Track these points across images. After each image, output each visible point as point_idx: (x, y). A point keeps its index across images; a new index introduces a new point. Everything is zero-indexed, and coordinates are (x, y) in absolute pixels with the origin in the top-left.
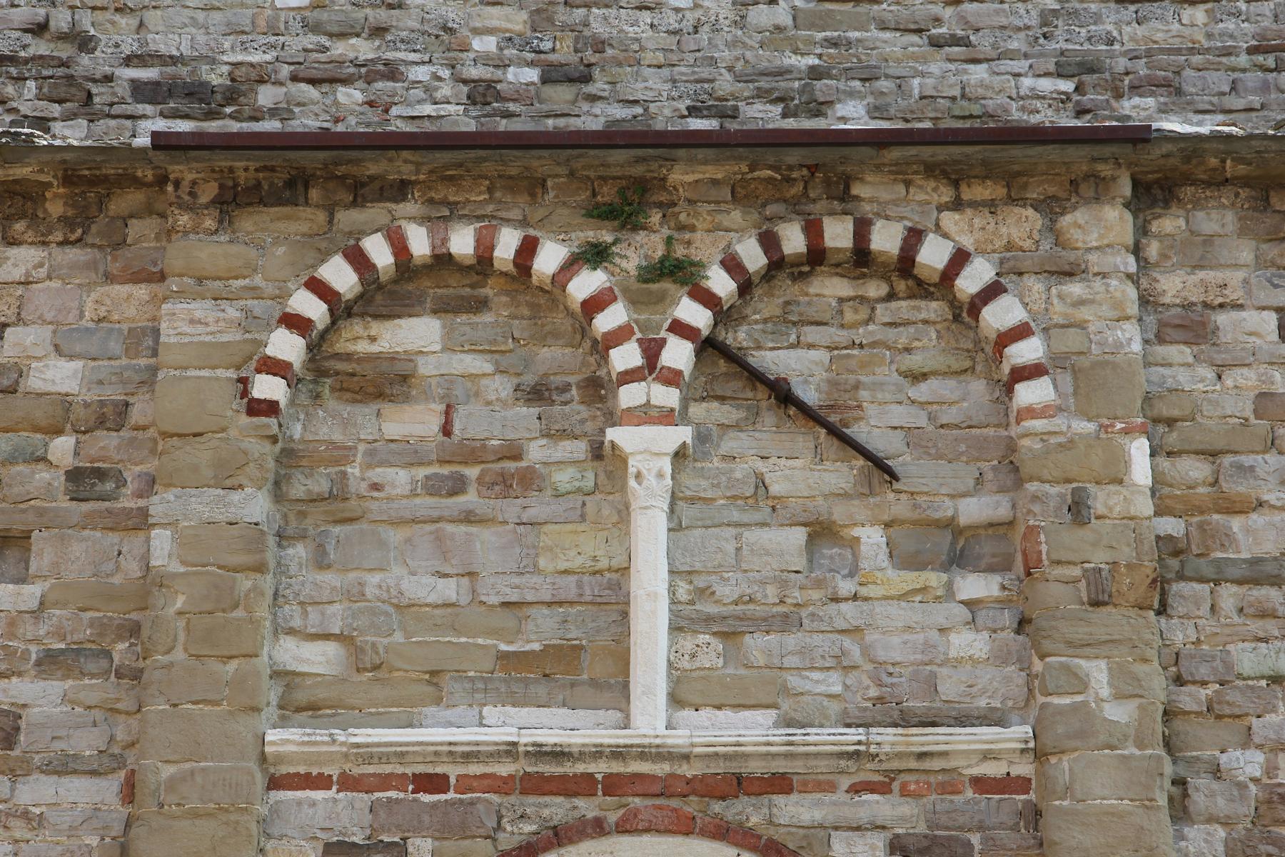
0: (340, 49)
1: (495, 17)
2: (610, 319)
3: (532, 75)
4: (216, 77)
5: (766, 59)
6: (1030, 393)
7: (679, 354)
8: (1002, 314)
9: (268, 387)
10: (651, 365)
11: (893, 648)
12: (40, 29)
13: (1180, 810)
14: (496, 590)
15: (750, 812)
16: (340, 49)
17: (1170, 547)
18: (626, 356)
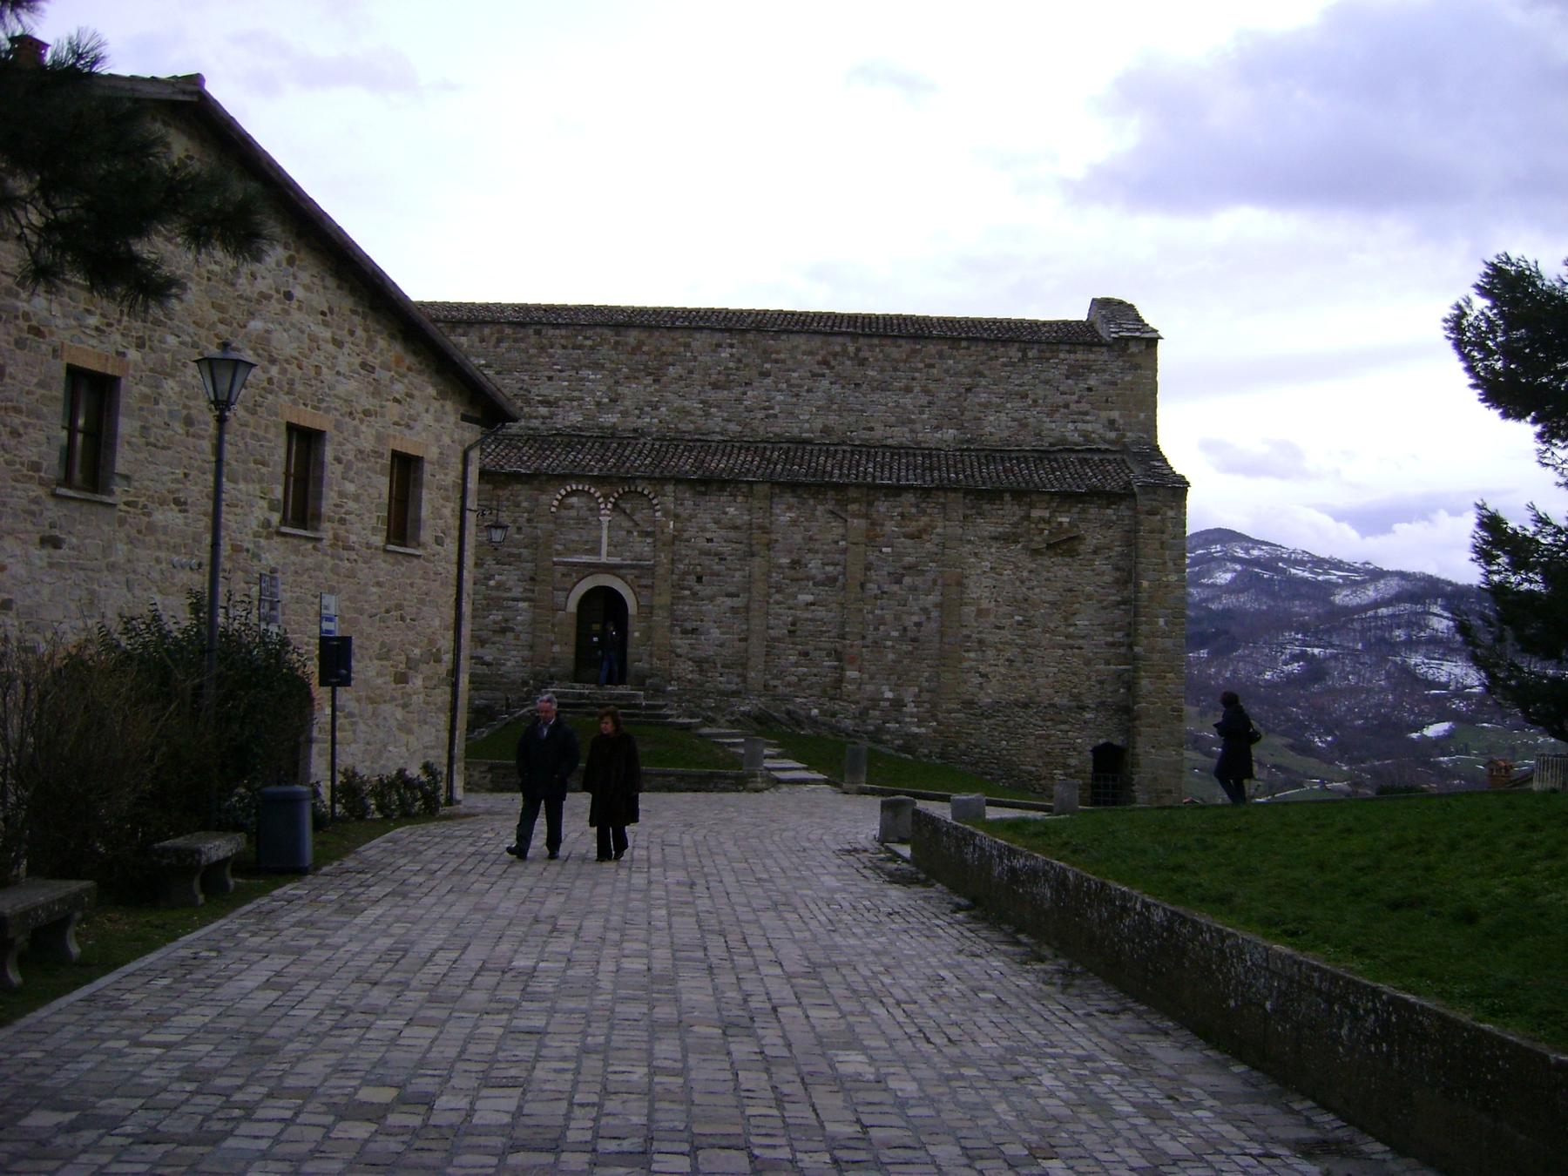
0: (574, 394)
1: (601, 388)
2: (601, 500)
3: (606, 400)
4: (551, 399)
5: (649, 398)
6: (658, 514)
7: (610, 506)
8: (655, 502)
9: (553, 509)
10: (606, 508)
11: (638, 549)
12: (521, 389)
13: (673, 573)
14: (585, 538)
15: (617, 572)
16: (574, 394)
17: (674, 536)
18: (602, 506)
